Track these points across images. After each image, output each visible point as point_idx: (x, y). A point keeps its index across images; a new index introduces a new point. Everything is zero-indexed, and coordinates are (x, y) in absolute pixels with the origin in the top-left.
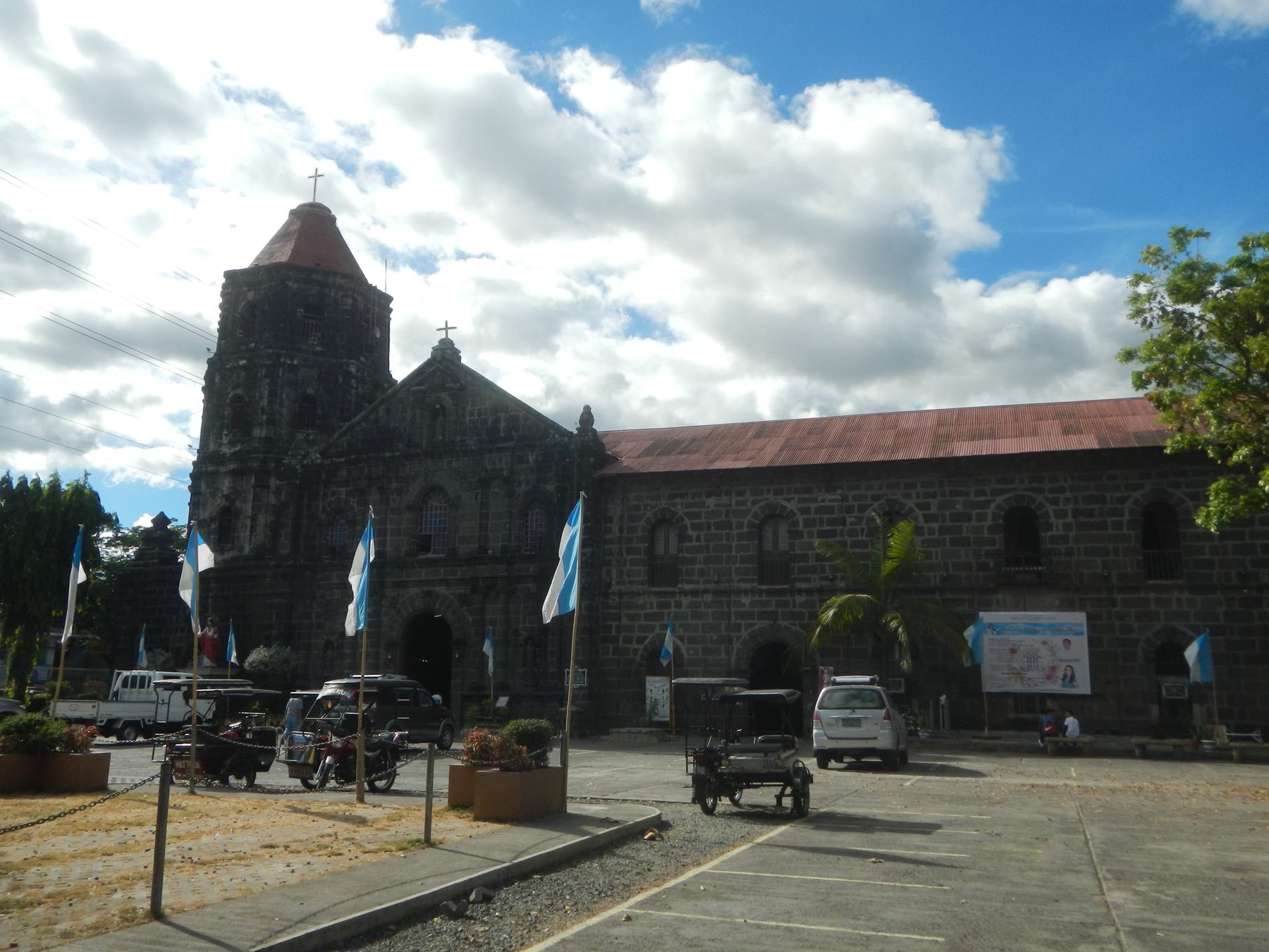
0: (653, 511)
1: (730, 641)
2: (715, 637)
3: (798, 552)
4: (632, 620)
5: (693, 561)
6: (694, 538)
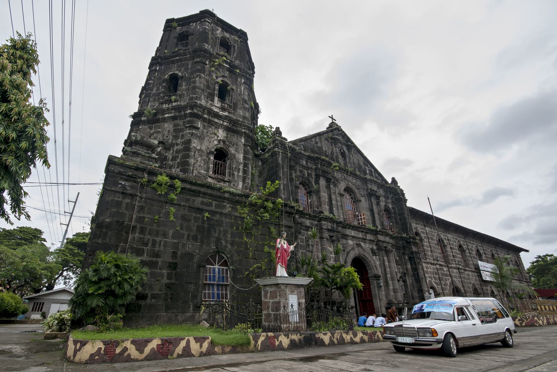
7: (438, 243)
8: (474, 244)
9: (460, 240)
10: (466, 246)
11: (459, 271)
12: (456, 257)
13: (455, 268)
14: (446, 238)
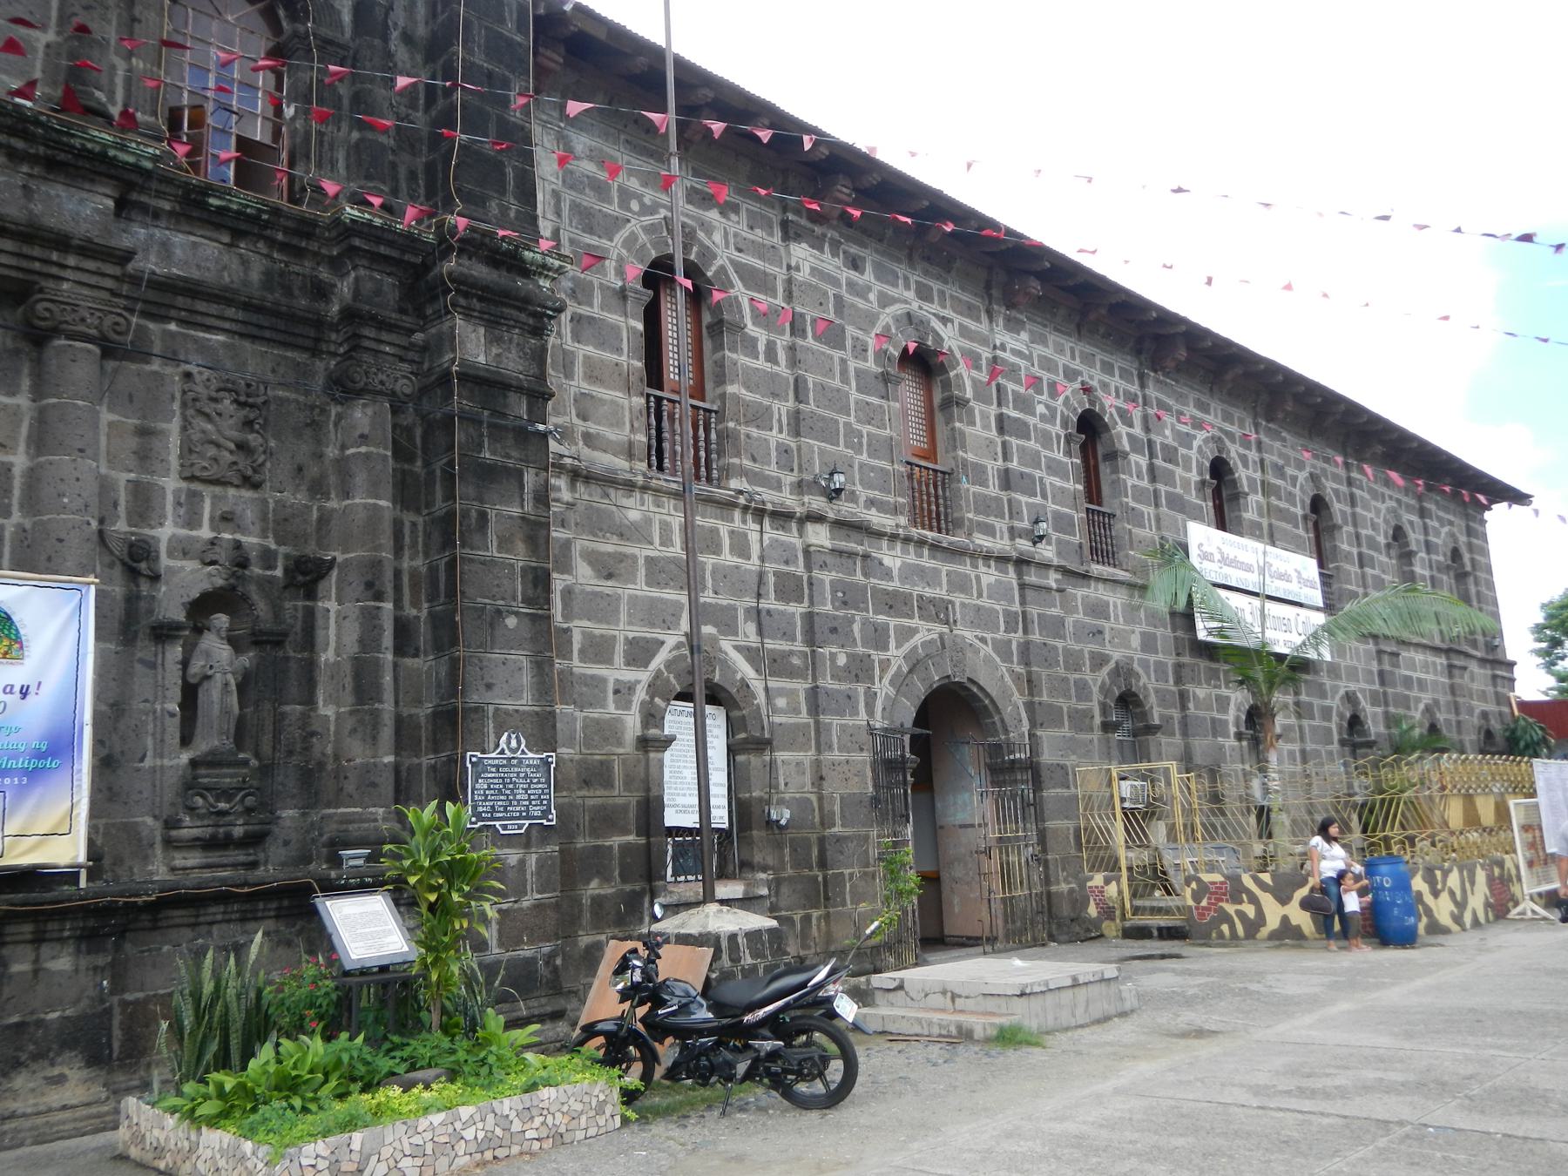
0: (647, 220)
1: (860, 670)
2: (842, 660)
3: (970, 457)
4: (610, 576)
5: (761, 417)
6: (761, 347)
7: (885, 378)
8: (1198, 425)
9: (1105, 386)
10: (1138, 430)
11: (1020, 575)
12: (1028, 485)
13: (1002, 560)
14: (986, 354)
